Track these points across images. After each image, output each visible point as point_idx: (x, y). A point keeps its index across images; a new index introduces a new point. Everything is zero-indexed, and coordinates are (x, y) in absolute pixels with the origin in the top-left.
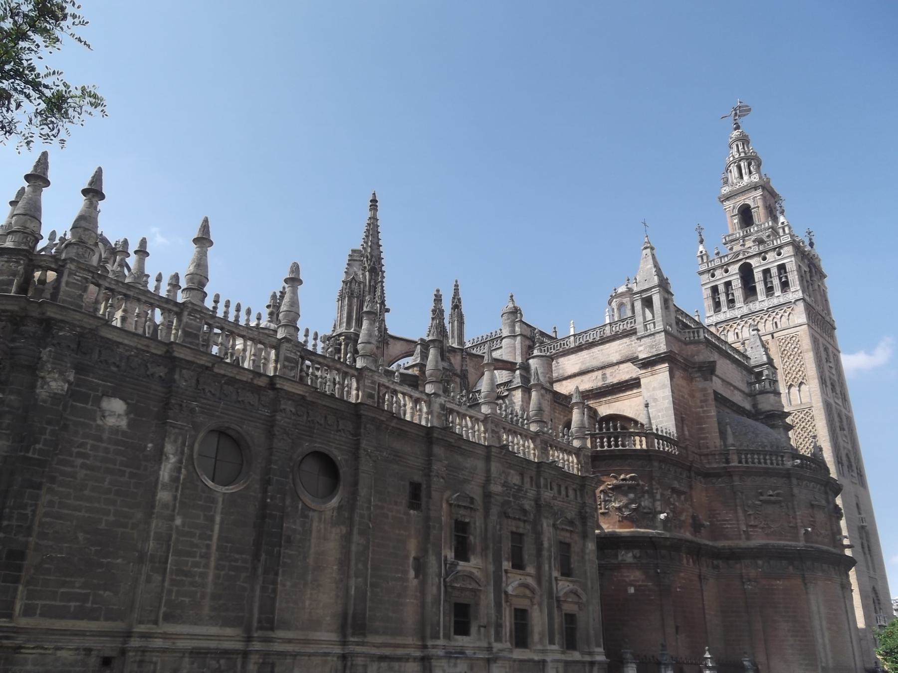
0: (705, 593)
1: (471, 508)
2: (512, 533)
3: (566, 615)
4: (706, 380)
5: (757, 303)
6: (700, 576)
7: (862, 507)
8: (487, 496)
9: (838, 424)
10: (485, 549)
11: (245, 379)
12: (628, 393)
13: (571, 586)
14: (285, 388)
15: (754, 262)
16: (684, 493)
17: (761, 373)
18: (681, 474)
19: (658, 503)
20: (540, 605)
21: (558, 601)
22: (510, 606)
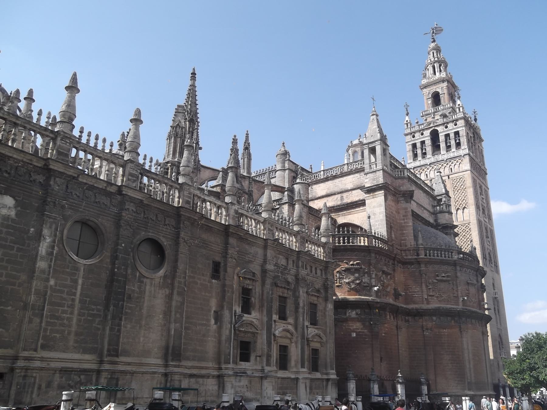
0: (399, 337)
1: (253, 280)
2: (280, 296)
3: (312, 349)
4: (407, 202)
5: (440, 155)
6: (397, 326)
7: (496, 285)
8: (264, 272)
9: (485, 234)
10: (262, 306)
11: (101, 187)
12: (357, 209)
13: (317, 331)
14: (129, 194)
15: (440, 129)
17: (441, 200)
18: (389, 262)
19: (373, 280)
20: (296, 343)
21: (308, 341)
22: (277, 343)
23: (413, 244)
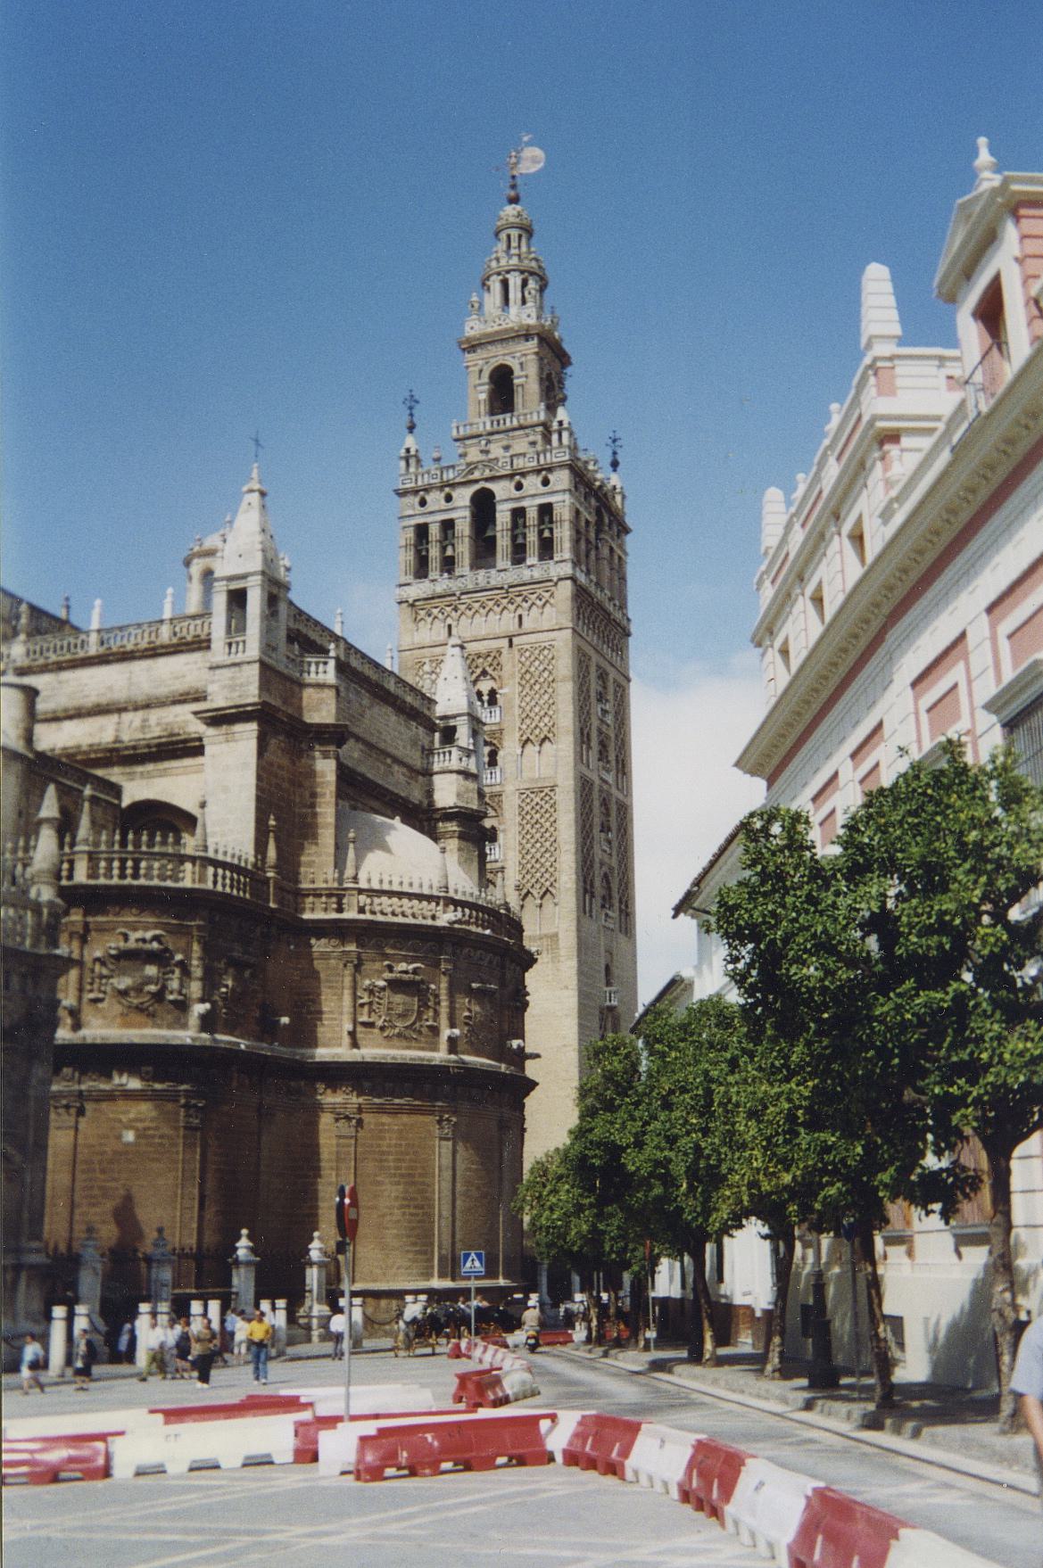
5: (493, 571)
7: (615, 971)
9: (597, 821)
15: (501, 490)
16: (248, 965)
17: (454, 729)
23: (330, 877)
